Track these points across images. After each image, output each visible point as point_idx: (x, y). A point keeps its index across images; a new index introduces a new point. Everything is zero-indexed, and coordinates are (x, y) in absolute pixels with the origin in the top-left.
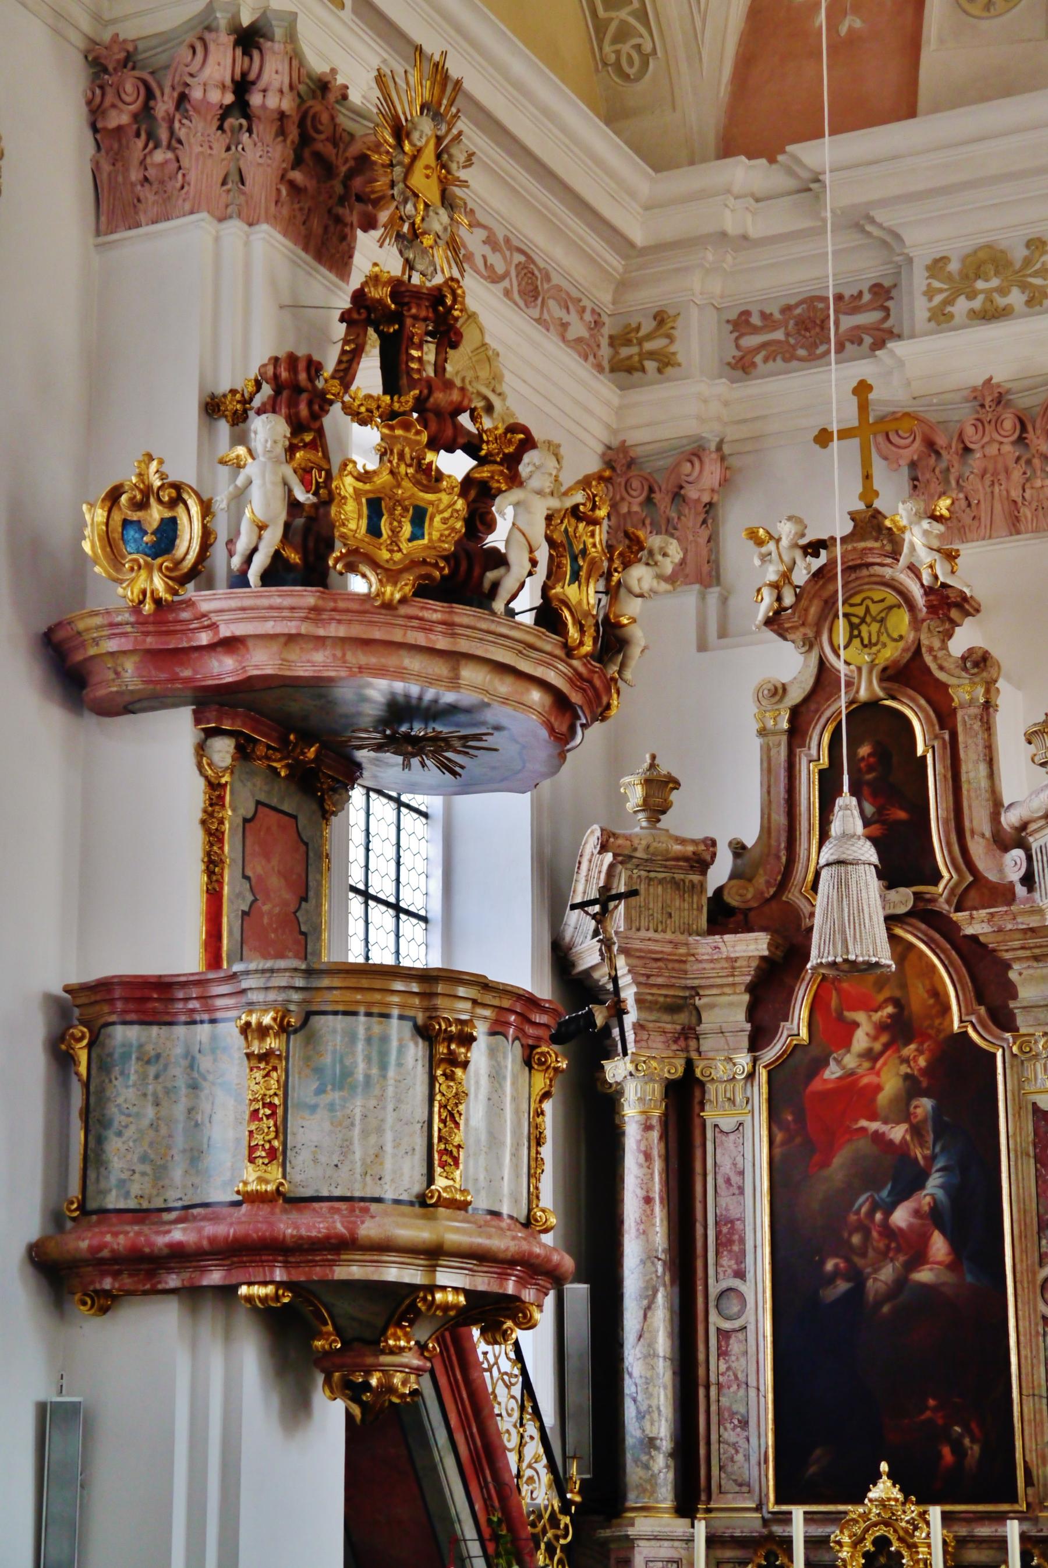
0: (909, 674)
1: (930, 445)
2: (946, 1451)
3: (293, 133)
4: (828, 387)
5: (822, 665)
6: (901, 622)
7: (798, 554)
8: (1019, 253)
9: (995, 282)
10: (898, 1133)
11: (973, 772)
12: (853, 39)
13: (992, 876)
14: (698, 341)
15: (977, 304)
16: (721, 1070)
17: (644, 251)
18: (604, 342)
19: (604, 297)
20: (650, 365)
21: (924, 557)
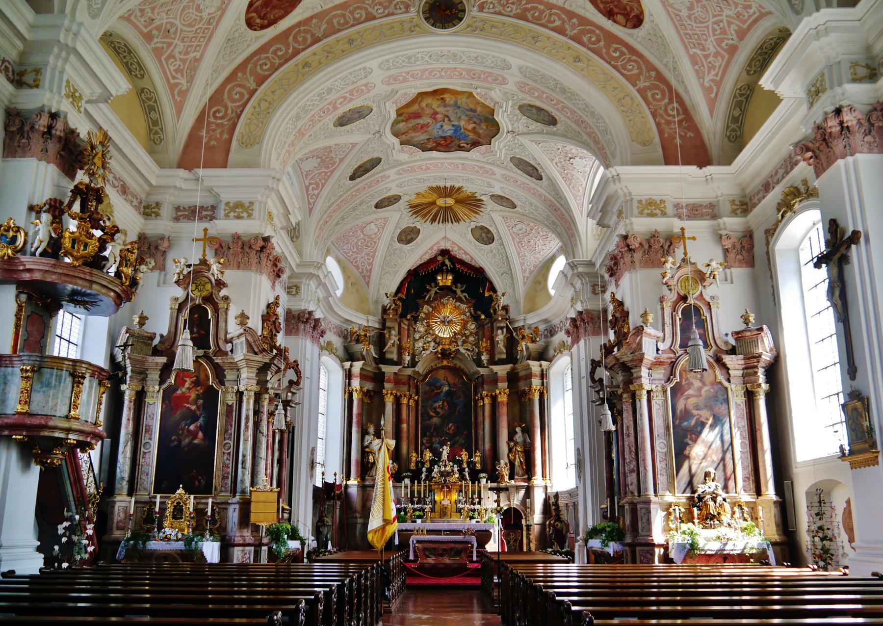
1: (221, 246)
2: (197, 483)
3: (63, 142)
4: (196, 228)
6: (209, 286)
8: (247, 204)
10: (194, 407)
11: (222, 324)
12: (214, 147)
14: (166, 211)
16: (151, 389)
19: (143, 196)
20: (153, 215)
21: (216, 272)
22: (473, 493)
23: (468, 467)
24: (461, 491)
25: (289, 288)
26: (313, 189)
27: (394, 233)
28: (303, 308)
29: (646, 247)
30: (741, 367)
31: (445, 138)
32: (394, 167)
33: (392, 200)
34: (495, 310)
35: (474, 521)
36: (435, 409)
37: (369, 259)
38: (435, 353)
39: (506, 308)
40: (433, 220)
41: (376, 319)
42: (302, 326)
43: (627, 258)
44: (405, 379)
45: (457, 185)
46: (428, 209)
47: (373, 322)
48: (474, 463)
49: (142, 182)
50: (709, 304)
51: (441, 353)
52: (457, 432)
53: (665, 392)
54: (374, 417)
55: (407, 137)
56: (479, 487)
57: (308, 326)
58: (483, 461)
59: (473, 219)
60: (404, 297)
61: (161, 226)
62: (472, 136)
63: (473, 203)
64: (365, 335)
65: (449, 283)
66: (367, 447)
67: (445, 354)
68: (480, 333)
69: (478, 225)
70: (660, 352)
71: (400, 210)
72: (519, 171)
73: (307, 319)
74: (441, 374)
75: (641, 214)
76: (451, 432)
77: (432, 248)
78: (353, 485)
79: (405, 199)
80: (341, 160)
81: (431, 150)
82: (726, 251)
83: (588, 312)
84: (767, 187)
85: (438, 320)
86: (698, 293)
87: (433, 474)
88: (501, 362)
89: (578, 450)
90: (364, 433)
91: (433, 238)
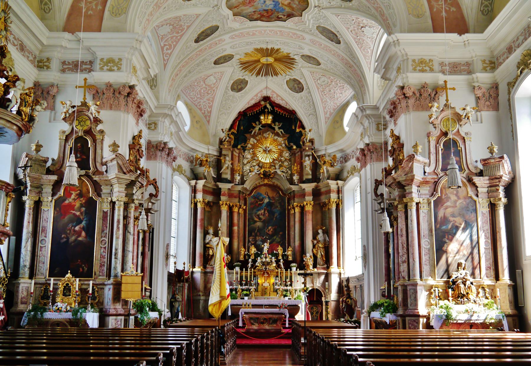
0: (89, 132)
1: (97, 92)
2: (81, 269)
4: (79, 78)
5: (73, 129)
6: (88, 122)
7: (70, 107)
8: (117, 60)
9: (112, 65)
10: (78, 213)
11: (99, 151)
13: (100, 170)
14: (55, 65)
15: (108, 68)
16: (46, 200)
17: (45, 46)
18: (36, 62)
19: (37, 53)
20: (45, 67)
21: (94, 112)
22: (286, 278)
23: (283, 258)
24: (277, 276)
25: (149, 124)
26: (167, 49)
27: (228, 83)
28: (160, 140)
29: (418, 95)
30: (487, 186)
31: (267, 11)
32: (229, 32)
33: (227, 58)
34: (304, 142)
35: (287, 298)
36: (258, 216)
37: (209, 103)
38: (259, 174)
39: (312, 141)
40: (258, 74)
41: (215, 148)
42: (159, 153)
43: (404, 103)
44: (236, 193)
45: (276, 47)
46: (254, 66)
47: (213, 151)
48: (287, 256)
49: (36, 42)
50: (464, 138)
51: (264, 174)
52: (275, 233)
53: (429, 204)
54: (213, 221)
55: (239, 10)
56: (291, 273)
57: (164, 153)
58: (294, 254)
59: (288, 73)
60: (235, 132)
61: (51, 76)
62: (287, 9)
63: (288, 61)
64: (207, 161)
65: (269, 122)
66: (208, 243)
67: (266, 175)
68: (293, 159)
69: (292, 78)
70: (426, 174)
71: (232, 66)
72: (323, 37)
73: (163, 148)
74: (263, 190)
75: (415, 70)
76: (270, 233)
77: (256, 95)
78: (197, 272)
79: (236, 57)
80: (188, 27)
81: (256, 20)
82: (478, 99)
83: (373, 144)
84: (510, 50)
85: (261, 150)
86: (455, 130)
87: (257, 264)
88: (308, 181)
89: (364, 246)
90: (206, 233)
91: (257, 88)
